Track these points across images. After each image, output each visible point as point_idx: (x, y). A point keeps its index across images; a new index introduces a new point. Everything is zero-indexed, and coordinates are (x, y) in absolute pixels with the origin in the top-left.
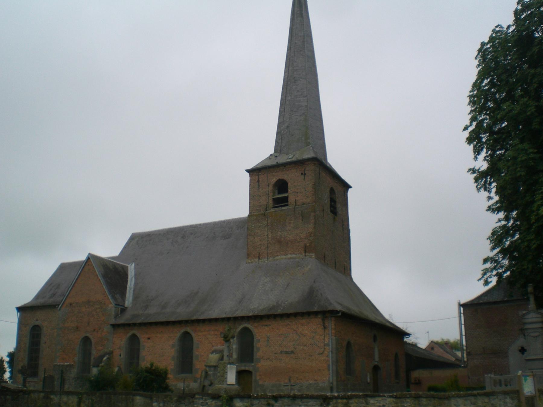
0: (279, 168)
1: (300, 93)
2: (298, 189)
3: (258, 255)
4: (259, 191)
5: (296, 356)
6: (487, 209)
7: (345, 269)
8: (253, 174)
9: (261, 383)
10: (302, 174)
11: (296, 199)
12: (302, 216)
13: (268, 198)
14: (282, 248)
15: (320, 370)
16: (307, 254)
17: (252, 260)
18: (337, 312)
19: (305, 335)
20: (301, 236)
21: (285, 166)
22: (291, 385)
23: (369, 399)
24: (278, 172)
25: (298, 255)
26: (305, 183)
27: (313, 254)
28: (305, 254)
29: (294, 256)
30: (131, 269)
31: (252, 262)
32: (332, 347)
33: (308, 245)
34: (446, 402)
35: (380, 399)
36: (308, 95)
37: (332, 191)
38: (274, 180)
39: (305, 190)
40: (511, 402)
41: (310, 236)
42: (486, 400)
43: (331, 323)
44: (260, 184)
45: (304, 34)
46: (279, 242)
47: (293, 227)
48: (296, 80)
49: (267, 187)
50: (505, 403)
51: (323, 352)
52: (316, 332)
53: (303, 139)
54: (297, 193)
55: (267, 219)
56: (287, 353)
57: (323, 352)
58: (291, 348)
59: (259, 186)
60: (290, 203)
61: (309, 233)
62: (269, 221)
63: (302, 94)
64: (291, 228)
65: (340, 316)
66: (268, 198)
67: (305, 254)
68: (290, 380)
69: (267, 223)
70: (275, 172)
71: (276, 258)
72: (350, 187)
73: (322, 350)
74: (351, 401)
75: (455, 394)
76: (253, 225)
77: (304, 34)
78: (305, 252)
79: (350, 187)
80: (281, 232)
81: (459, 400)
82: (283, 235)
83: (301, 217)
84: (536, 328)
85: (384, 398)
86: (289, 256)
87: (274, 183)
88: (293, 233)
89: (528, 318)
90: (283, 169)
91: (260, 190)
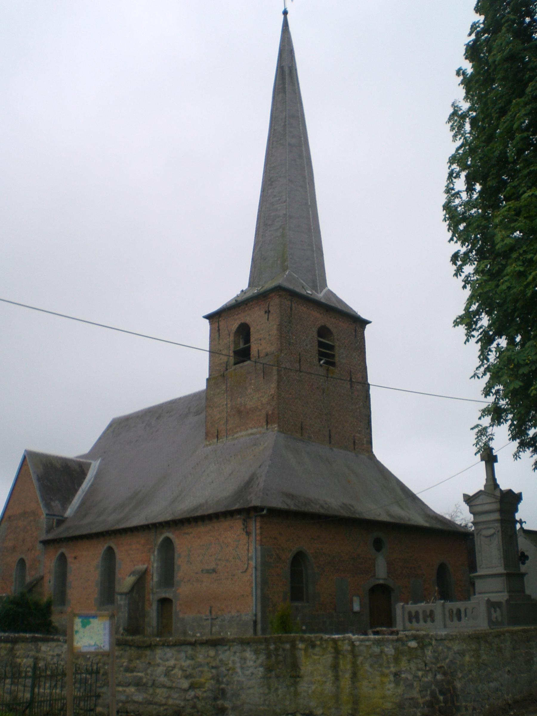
0: (241, 308)
1: (277, 199)
2: (261, 334)
3: (216, 434)
4: (219, 344)
5: (218, 576)
6: (453, 325)
7: (354, 442)
8: (213, 321)
9: (181, 616)
10: (266, 312)
11: (260, 348)
12: (264, 372)
13: (229, 352)
14: (242, 420)
15: (243, 595)
16: (269, 426)
17: (211, 442)
18: (262, 509)
19: (228, 546)
20: (262, 401)
21: (246, 304)
22: (212, 619)
23: (40, 644)
24: (240, 313)
25: (258, 429)
26: (269, 324)
27: (276, 425)
28: (267, 426)
29: (255, 430)
30: (95, 466)
31: (210, 445)
32: (256, 562)
33: (270, 413)
34: (148, 652)
35: (54, 644)
36: (288, 199)
37: (323, 332)
38: (235, 326)
39: (269, 335)
40: (254, 657)
41: (273, 400)
42: (212, 653)
43: (255, 526)
44: (221, 334)
45: (286, 114)
46: (239, 412)
47: (254, 389)
48: (273, 182)
49: (228, 337)
50: (244, 659)
51: (247, 569)
52: (240, 540)
53: (279, 262)
54: (260, 340)
55: (226, 381)
56: (208, 572)
57: (247, 569)
58: (212, 566)
59: (219, 336)
60: (253, 355)
61: (271, 395)
62: (229, 384)
63: (279, 200)
64: (251, 390)
65: (265, 514)
66: (229, 352)
67: (267, 426)
68: (211, 612)
69: (227, 387)
70: (237, 315)
71: (236, 436)
72: (367, 322)
73: (246, 566)
74: (17, 647)
75: (160, 641)
76: (212, 392)
77: (286, 114)
78: (267, 423)
79: (367, 322)
80: (241, 398)
81: (167, 650)
82: (243, 402)
83: (262, 374)
84: (488, 521)
85: (59, 643)
86: (250, 431)
87: (235, 330)
88: (254, 397)
89: (475, 505)
90: (245, 308)
91: (221, 341)
